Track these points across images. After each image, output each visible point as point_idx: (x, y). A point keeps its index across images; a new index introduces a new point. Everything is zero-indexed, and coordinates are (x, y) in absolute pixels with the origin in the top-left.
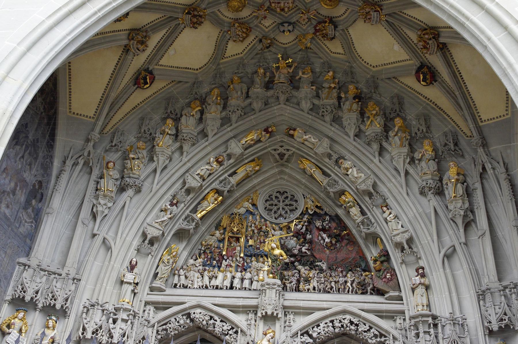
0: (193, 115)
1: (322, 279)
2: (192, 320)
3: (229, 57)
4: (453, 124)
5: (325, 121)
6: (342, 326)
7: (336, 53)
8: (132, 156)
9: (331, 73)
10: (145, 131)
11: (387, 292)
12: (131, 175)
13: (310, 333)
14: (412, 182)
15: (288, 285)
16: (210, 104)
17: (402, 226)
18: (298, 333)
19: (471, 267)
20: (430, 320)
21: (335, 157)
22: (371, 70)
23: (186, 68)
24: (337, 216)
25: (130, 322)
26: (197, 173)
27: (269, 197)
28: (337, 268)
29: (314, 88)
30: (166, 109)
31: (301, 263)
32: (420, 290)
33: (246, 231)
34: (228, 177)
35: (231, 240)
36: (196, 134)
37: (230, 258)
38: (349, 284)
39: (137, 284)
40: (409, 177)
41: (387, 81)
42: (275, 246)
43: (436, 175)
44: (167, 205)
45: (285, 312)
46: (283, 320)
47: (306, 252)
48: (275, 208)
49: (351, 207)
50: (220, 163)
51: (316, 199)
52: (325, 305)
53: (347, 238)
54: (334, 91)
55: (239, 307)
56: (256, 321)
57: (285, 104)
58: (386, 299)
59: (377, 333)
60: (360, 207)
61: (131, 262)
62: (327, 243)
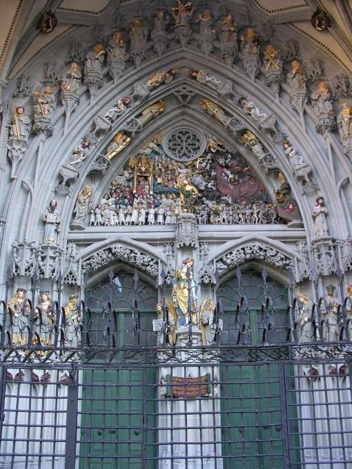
0: (97, 59)
1: (231, 212)
2: (114, 254)
4: (344, 68)
6: (253, 252)
8: (40, 100)
9: (229, 17)
11: (291, 221)
12: (42, 120)
13: (224, 260)
14: (310, 121)
15: (200, 219)
16: (113, 48)
18: (213, 261)
20: (330, 243)
21: (237, 98)
24: (239, 154)
25: (57, 259)
26: (106, 115)
29: (214, 31)
30: (69, 53)
32: (320, 218)
33: (154, 170)
35: (141, 179)
36: (101, 77)
37: (141, 196)
38: (255, 215)
39: (59, 224)
40: (306, 116)
41: (282, 26)
42: (187, 182)
43: (332, 115)
45: (200, 243)
46: (198, 250)
49: (254, 145)
50: (126, 105)
51: (218, 138)
52: (236, 234)
54: (234, 34)
55: (157, 240)
56: (173, 252)
57: (186, 47)
58: (289, 227)
59: (283, 257)
60: (263, 145)
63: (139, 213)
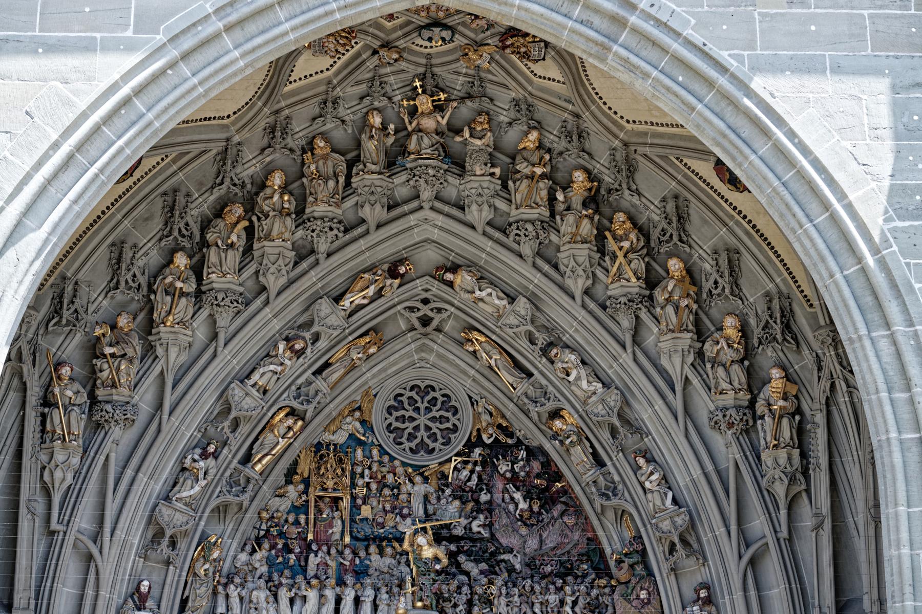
3: (300, 79)
5: (520, 256)
7: (544, 78)
8: (108, 350)
9: (534, 136)
10: (127, 282)
12: (115, 398)
17: (675, 501)
19: (794, 586)
21: (542, 339)
22: (621, 128)
23: (205, 119)
24: (541, 450)
26: (251, 382)
27: (395, 398)
28: (542, 564)
29: (497, 171)
31: (469, 556)
34: (313, 377)
44: (196, 457)
47: (479, 533)
48: (409, 426)
53: (562, 499)
54: (541, 185)
57: (432, 208)
60: (592, 446)
61: (138, 589)
62: (522, 510)
63: (321, 596)
